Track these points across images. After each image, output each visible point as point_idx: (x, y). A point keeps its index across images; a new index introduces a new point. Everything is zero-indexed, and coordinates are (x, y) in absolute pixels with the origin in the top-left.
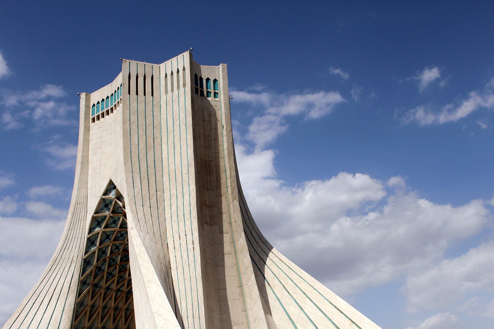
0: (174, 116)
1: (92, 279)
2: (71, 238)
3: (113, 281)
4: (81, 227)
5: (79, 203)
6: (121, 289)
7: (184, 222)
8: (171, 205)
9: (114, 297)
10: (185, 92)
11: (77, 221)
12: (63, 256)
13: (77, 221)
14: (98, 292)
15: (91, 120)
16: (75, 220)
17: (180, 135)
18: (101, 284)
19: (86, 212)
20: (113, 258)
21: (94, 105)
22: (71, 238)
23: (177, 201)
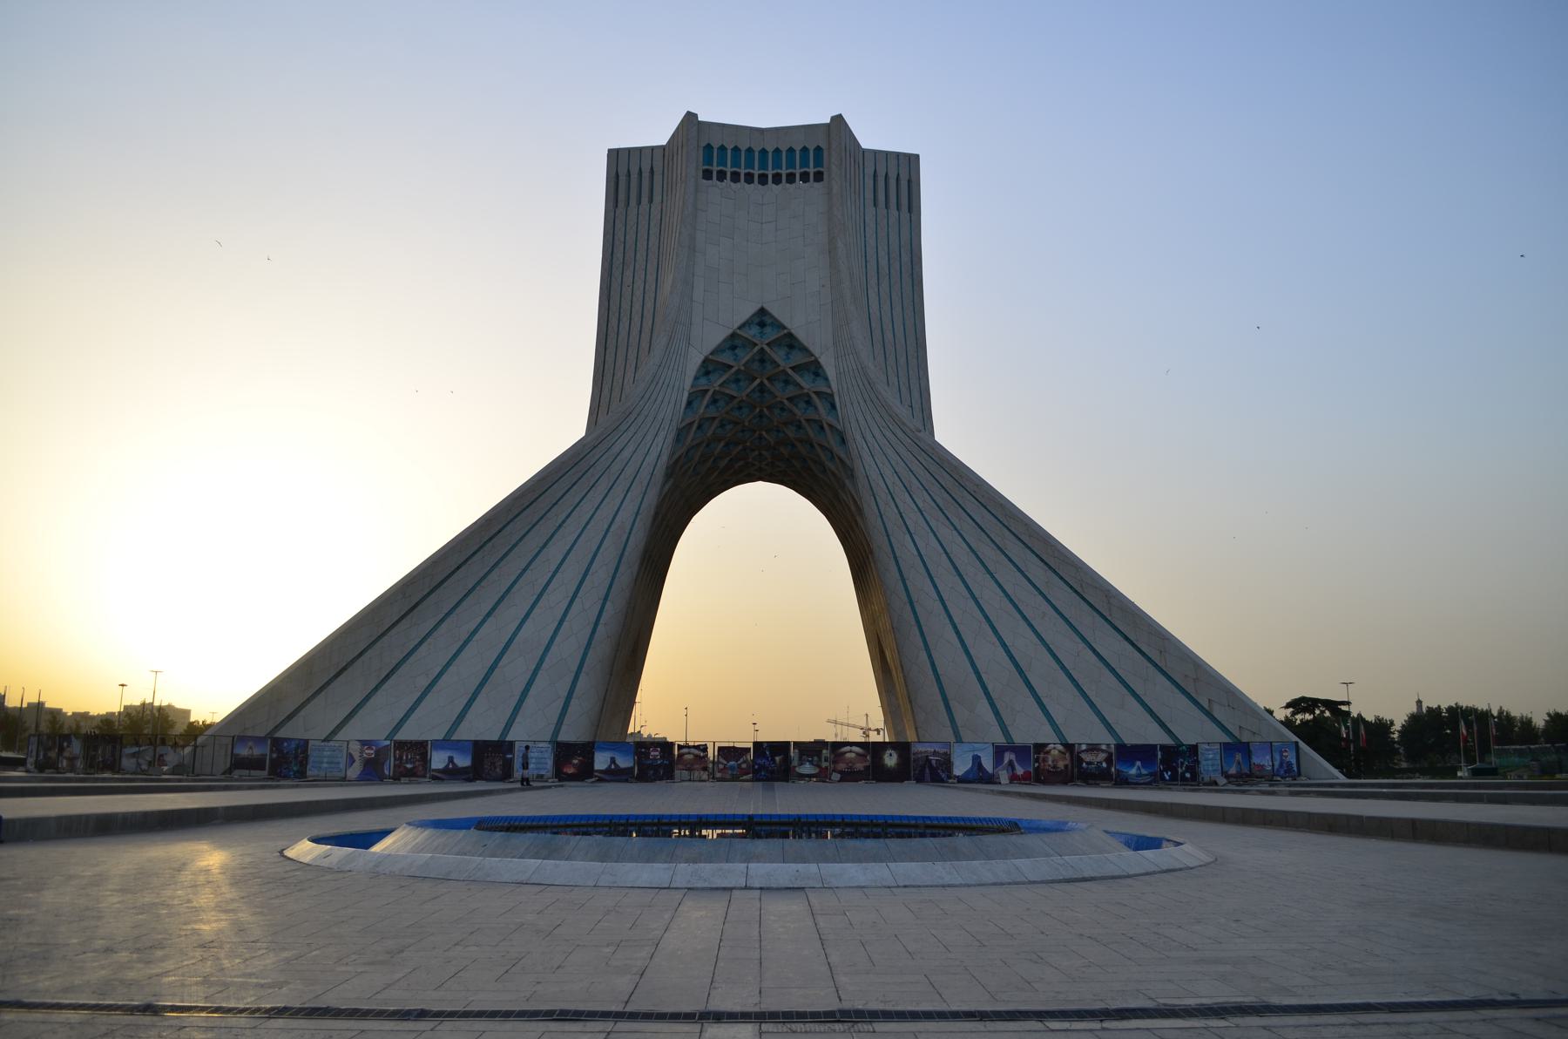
12: (645, 412)
21: (709, 147)
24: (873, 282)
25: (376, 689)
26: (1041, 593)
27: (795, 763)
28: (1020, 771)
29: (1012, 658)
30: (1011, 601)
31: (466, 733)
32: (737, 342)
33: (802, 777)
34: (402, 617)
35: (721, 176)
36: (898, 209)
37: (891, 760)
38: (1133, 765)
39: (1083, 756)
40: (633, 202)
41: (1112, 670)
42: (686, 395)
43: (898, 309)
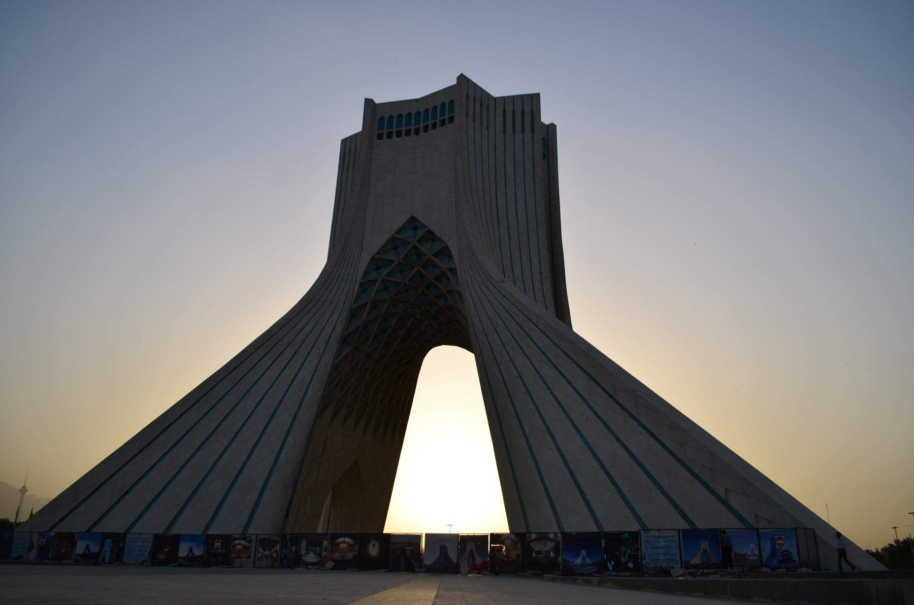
2: (337, 276)
15: (376, 136)
21: (382, 118)
22: (337, 276)
25: (118, 501)
26: (585, 401)
27: (303, 552)
28: (479, 561)
29: (565, 461)
30: (564, 410)
31: (102, 528)
33: (307, 564)
34: (141, 451)
35: (390, 136)
36: (523, 132)
37: (373, 550)
38: (578, 555)
39: (533, 545)
40: (351, 169)
41: (641, 466)
42: (358, 284)
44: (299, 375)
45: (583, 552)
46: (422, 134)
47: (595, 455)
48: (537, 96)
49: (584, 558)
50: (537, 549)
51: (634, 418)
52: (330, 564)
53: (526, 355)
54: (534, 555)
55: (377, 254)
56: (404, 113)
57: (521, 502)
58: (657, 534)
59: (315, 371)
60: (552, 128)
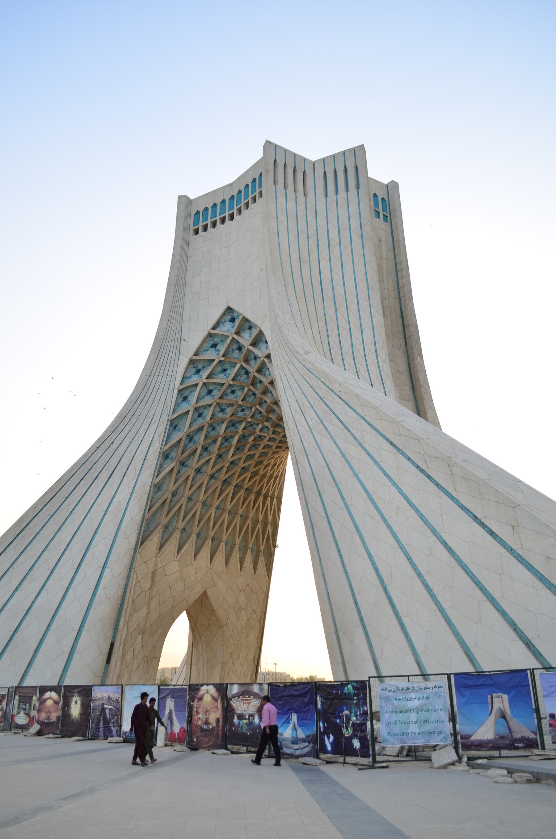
0: (340, 225)
1: (180, 451)
3: (208, 461)
4: (170, 374)
5: (168, 339)
6: (216, 475)
7: (367, 367)
8: (340, 342)
9: (205, 485)
10: (358, 195)
11: (164, 364)
12: (138, 413)
13: (164, 364)
14: (184, 473)
15: (192, 232)
16: (161, 362)
17: (352, 249)
18: (189, 462)
19: (178, 354)
20: (214, 425)
21: (198, 213)
23: (351, 338)
24: (324, 253)
26: (394, 484)
30: (372, 501)
32: (216, 340)
36: (347, 190)
43: (348, 267)
44: (115, 499)
45: (294, 717)
46: (236, 217)
47: (409, 559)
48: (362, 147)
49: (295, 729)
50: (239, 711)
51: (452, 498)
52: (36, 727)
53: (332, 437)
54: (236, 720)
55: (195, 355)
56: (218, 202)
57: (337, 632)
58: (403, 683)
59: (132, 493)
60: (392, 188)
